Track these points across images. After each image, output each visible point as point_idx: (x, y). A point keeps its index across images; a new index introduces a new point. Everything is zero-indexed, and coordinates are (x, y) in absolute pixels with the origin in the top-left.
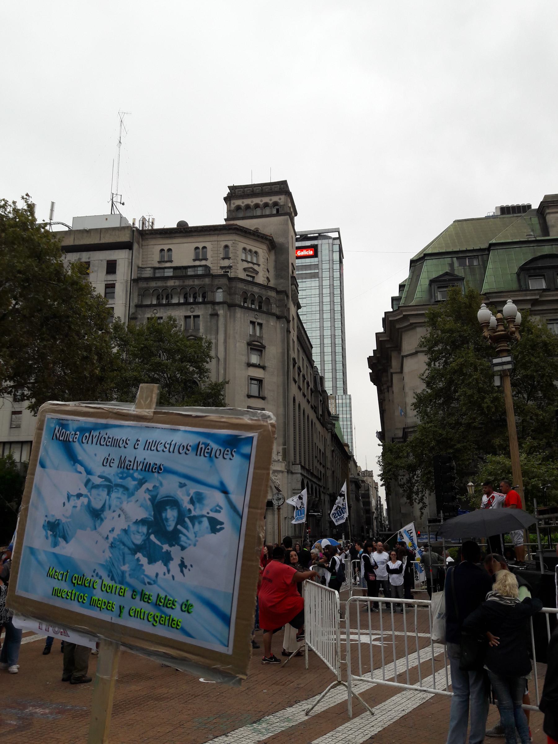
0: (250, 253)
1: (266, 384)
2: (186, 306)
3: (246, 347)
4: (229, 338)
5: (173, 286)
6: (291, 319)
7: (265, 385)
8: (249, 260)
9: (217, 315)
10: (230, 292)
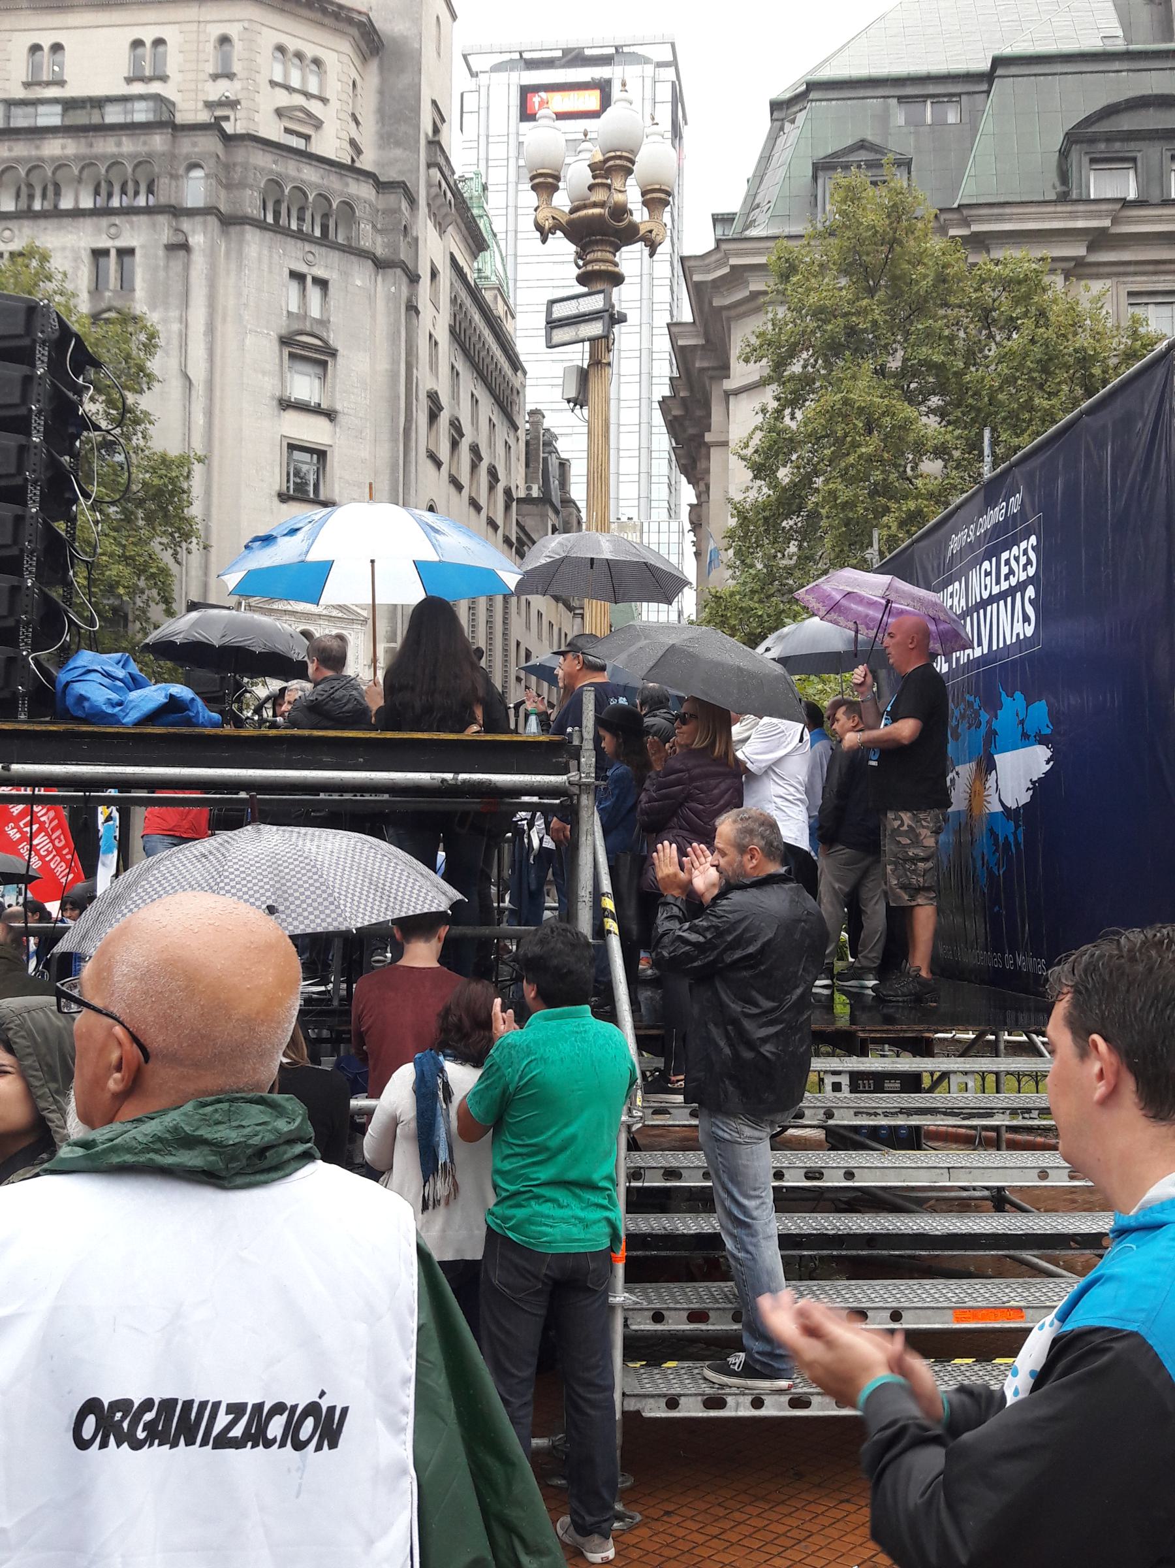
0: (296, 61)
1: (335, 461)
2: (95, 219)
3: (276, 345)
4: (224, 320)
5: (59, 158)
6: (425, 273)
7: (335, 464)
8: (295, 82)
9: (185, 247)
10: (226, 178)
